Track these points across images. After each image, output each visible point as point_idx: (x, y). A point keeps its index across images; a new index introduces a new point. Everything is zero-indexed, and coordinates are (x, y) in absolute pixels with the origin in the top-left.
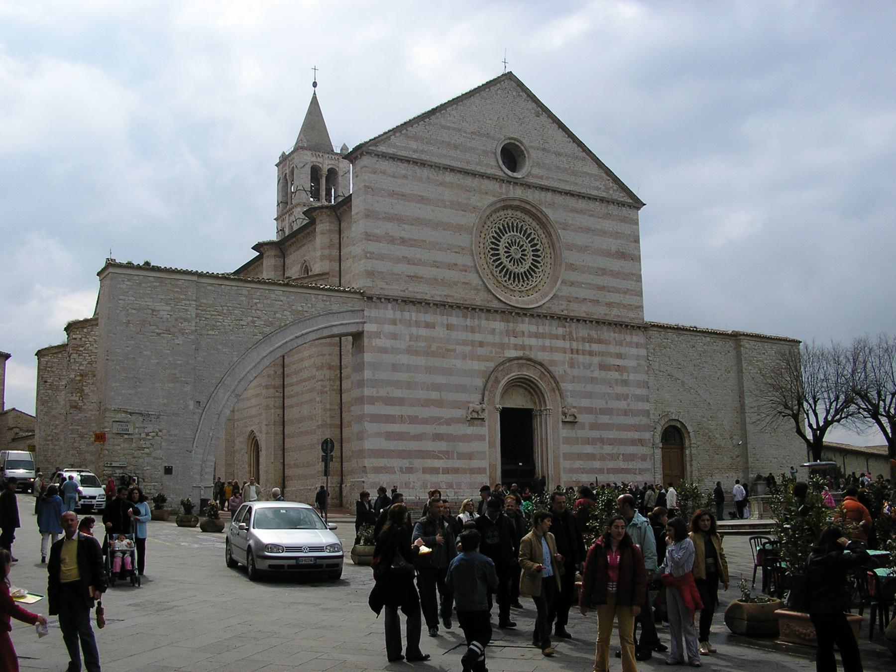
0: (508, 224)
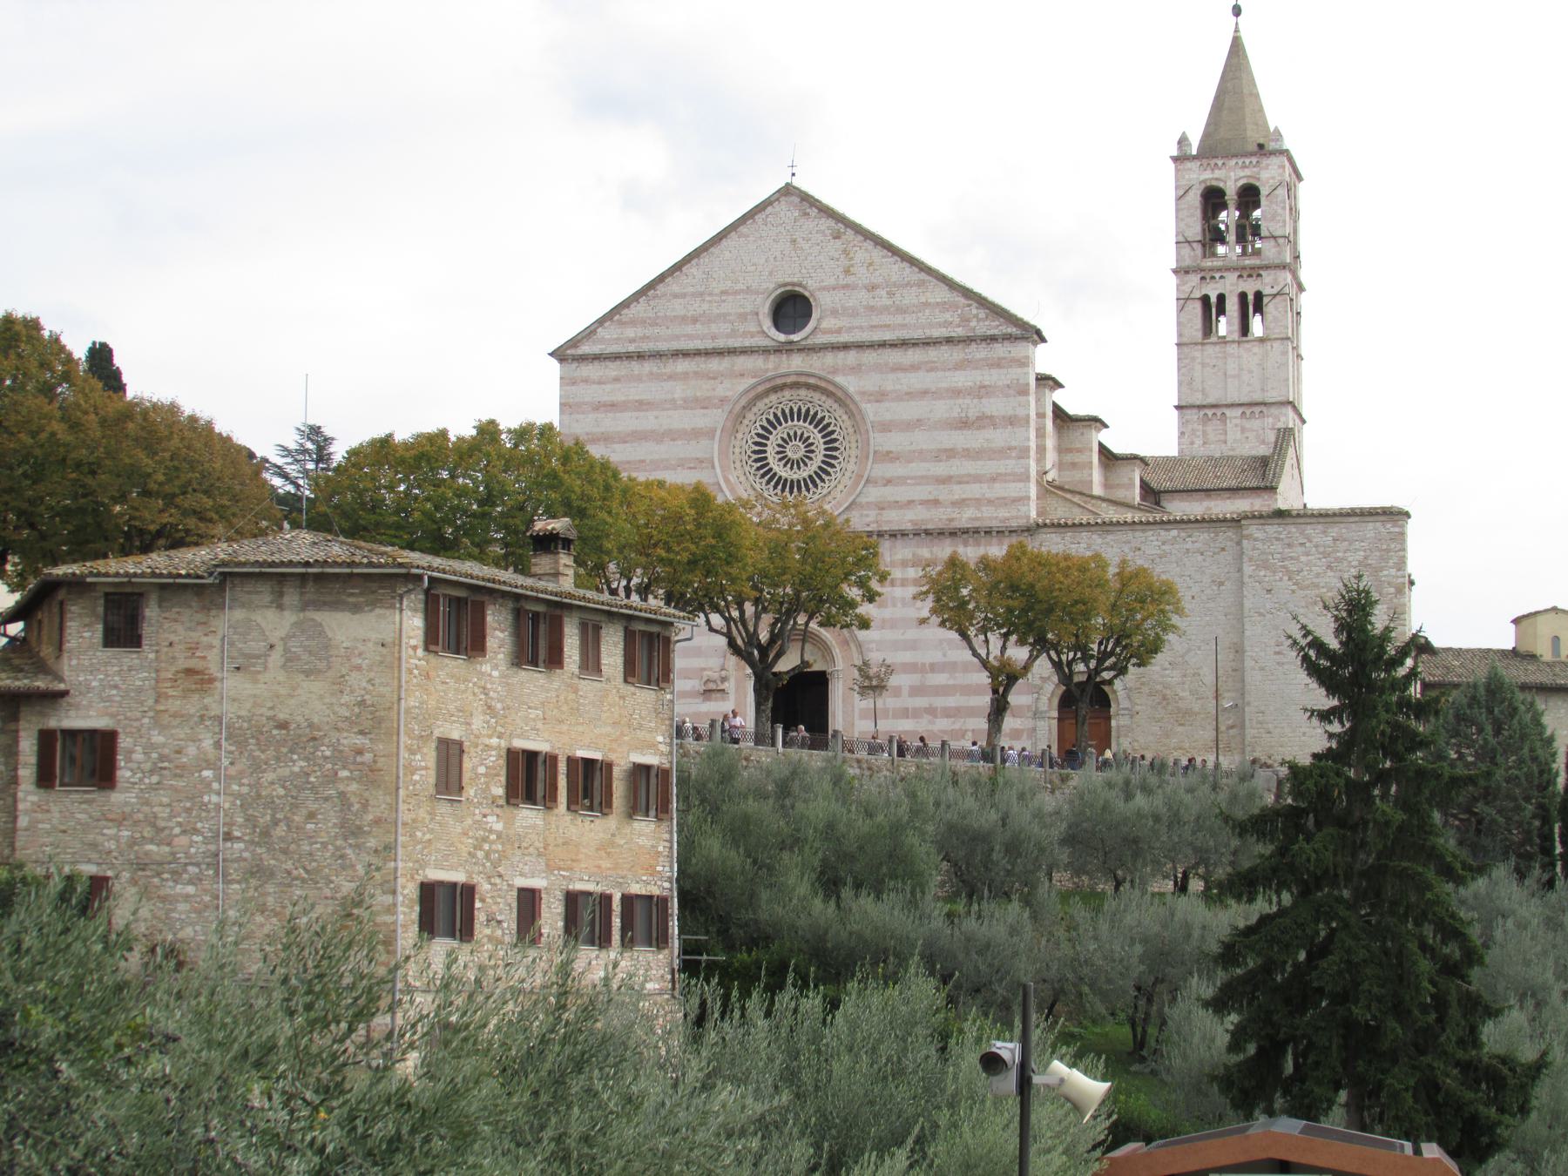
0: (783, 412)
